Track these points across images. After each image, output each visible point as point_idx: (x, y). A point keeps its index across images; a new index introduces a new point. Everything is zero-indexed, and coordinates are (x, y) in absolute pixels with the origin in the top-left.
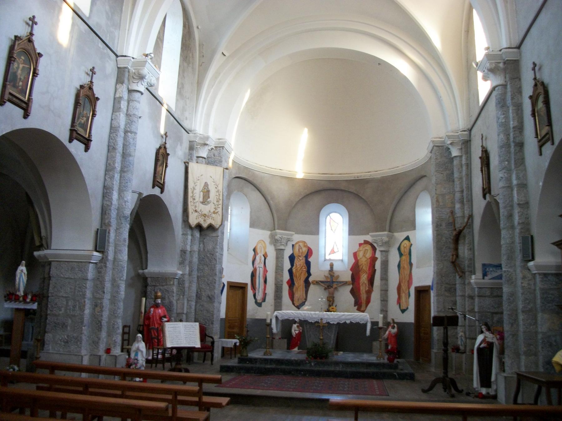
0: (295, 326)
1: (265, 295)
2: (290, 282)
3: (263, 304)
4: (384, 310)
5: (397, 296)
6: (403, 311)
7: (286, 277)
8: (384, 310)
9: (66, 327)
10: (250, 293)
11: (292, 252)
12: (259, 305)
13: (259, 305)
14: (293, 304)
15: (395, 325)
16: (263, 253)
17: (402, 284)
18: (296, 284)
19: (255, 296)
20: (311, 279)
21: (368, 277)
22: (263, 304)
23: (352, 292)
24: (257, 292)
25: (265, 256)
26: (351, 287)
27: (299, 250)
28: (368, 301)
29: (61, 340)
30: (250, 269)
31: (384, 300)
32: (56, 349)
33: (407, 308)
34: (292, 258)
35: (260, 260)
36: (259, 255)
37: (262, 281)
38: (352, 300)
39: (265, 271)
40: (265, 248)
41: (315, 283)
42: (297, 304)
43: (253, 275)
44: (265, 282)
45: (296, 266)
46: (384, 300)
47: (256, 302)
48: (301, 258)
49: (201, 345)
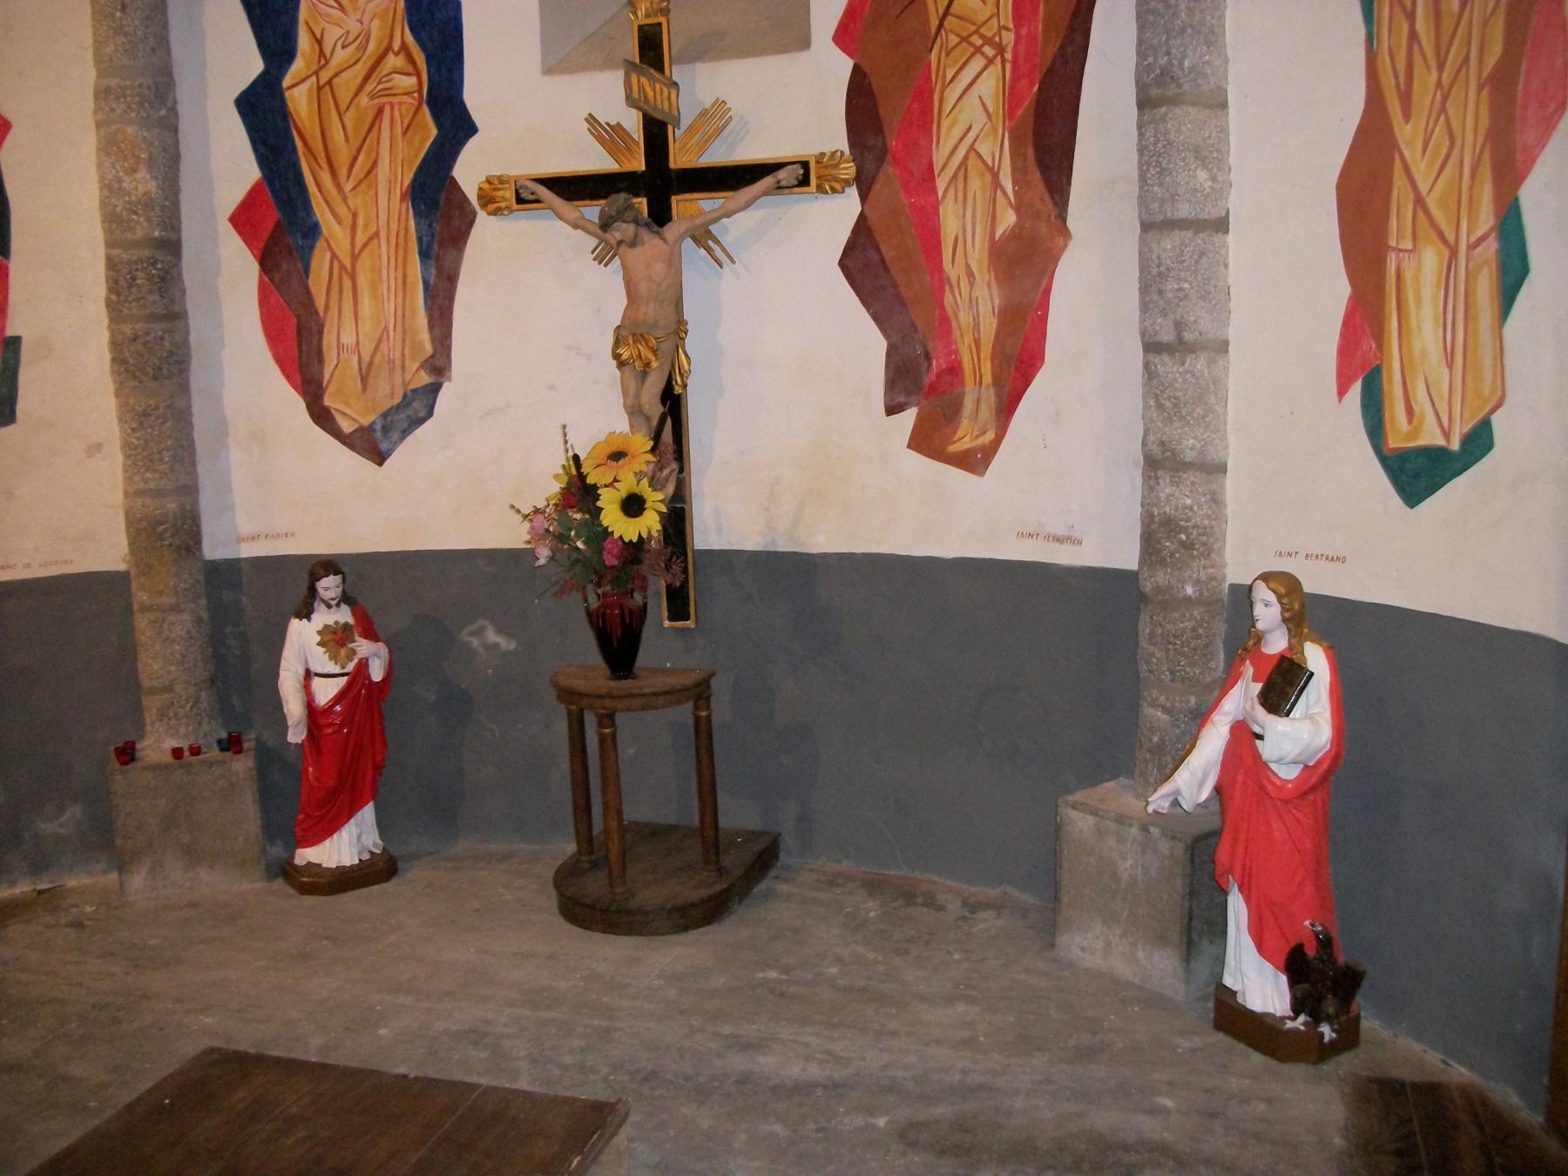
0: (303, 640)
2: (272, 216)
4: (1173, 462)
5: (1338, 290)
6: (1417, 474)
7: (227, 165)
8: (1173, 462)
14: (322, 417)
15: (1316, 658)
17: (1406, 133)
20: (469, 171)
21: (1012, 97)
23: (863, 262)
26: (846, 208)
28: (1020, 362)
31: (1175, 346)
33: (1479, 441)
38: (864, 346)
42: (352, 414)
45: (323, 57)
46: (1175, 346)
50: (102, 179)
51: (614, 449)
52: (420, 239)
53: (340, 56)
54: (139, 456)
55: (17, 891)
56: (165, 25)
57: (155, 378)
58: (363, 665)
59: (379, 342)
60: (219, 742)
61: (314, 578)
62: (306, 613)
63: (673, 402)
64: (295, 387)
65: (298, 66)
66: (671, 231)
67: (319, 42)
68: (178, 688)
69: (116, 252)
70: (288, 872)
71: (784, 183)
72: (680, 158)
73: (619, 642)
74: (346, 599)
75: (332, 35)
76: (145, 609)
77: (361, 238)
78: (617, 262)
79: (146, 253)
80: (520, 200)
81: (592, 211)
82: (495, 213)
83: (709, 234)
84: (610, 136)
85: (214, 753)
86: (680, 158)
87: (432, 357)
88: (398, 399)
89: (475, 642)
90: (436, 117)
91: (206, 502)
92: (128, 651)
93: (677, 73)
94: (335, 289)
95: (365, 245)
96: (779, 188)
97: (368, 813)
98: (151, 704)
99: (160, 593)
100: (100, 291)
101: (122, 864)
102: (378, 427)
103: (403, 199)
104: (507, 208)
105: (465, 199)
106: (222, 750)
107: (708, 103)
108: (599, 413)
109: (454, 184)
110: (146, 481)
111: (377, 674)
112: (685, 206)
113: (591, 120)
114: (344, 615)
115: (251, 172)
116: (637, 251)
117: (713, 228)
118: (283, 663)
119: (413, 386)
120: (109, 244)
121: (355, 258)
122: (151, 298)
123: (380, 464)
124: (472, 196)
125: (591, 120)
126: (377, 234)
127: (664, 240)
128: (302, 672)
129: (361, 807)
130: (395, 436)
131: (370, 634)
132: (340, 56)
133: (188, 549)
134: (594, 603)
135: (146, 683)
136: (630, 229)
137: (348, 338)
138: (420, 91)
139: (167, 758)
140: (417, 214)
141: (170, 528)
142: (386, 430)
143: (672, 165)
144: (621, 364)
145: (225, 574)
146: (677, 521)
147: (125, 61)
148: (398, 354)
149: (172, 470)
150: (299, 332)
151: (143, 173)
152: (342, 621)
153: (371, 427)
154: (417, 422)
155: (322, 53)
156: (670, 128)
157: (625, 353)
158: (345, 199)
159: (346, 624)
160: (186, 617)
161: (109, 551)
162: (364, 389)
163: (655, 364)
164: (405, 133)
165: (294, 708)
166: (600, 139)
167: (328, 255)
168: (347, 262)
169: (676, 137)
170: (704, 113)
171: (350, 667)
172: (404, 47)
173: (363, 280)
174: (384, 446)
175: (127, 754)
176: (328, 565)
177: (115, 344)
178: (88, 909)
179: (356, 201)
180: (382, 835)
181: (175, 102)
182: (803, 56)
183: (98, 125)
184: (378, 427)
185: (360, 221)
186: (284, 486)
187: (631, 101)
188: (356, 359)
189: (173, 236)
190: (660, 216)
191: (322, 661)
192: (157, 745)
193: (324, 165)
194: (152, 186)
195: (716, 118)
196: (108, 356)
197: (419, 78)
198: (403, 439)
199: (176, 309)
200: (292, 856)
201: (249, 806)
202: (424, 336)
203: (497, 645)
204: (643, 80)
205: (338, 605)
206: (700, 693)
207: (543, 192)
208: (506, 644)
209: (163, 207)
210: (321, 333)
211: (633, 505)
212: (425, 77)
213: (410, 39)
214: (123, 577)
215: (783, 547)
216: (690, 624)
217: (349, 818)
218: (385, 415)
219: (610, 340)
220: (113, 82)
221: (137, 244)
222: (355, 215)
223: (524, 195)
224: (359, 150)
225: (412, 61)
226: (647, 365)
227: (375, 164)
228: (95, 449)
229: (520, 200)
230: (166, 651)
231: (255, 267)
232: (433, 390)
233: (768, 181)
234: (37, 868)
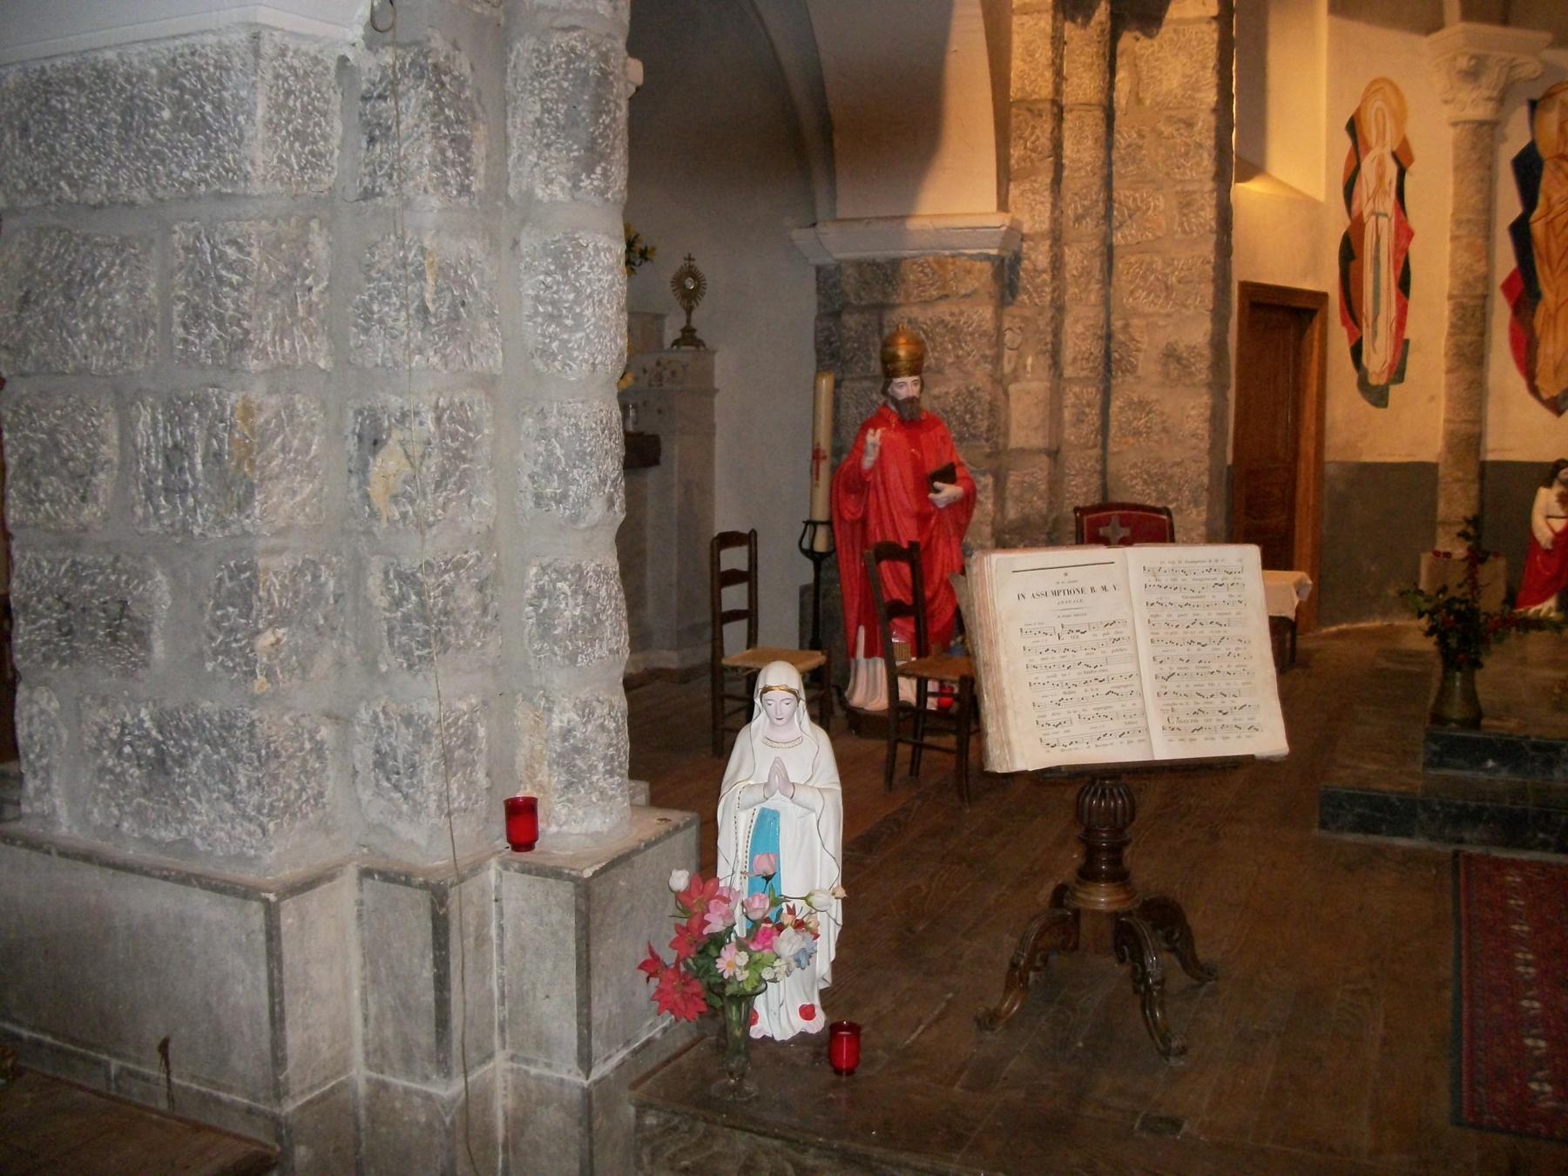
0: (1546, 498)
1: (1402, 347)
3: (1394, 390)
7: (1506, 261)
9: (141, 637)
10: (1339, 340)
12: (1378, 397)
13: (1378, 397)
14: (1534, 390)
16: (1390, 145)
19: (1357, 352)
22: (1394, 390)
24: (1366, 333)
25: (1402, 160)
29: (117, 745)
30: (1337, 224)
32: (97, 817)
34: (1528, 168)
35: (1381, 177)
39: (1404, 233)
40: (1400, 118)
42: (1549, 390)
43: (1350, 252)
44: (1404, 284)
45: (1550, 207)
47: (1363, 384)
49: (1291, 737)
62: (1549, 485)
65: (1537, 212)
75: (1556, 197)
77: (1561, 301)
121: (1557, 310)
132: (1559, 208)
137: (1550, 351)
141: (1468, 441)
161: (1431, 449)
228: (1432, 399)
234: (1385, 613)
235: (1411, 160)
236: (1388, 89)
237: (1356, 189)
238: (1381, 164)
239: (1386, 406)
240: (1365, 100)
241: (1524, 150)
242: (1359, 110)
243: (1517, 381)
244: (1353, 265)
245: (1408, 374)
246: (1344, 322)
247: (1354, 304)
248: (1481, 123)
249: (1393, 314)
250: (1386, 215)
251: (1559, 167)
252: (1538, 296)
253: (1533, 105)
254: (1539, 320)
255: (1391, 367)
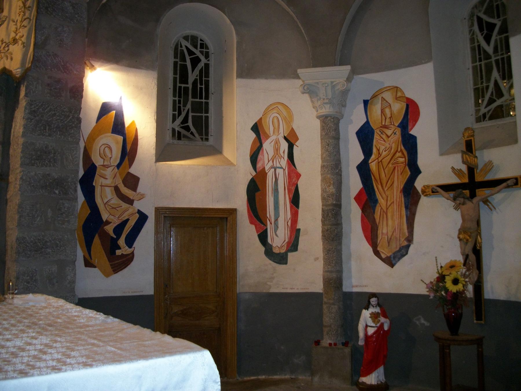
2: (365, 197)
3: (290, 254)
7: (354, 183)
10: (246, 232)
11: (365, 120)
14: (377, 253)
16: (283, 131)
18: (381, 201)
19: (263, 237)
20: (419, 184)
22: (290, 254)
25: (291, 141)
27: (382, 111)
34: (365, 136)
35: (277, 150)
36: (273, 138)
37: (284, 199)
39: (293, 174)
40: (289, 119)
41: (429, 191)
44: (295, 201)
45: (379, 154)
47: (269, 252)
48: (389, 132)
50: (322, 188)
51: (452, 264)
52: (405, 203)
53: (384, 154)
54: (327, 261)
55: (286, 377)
56: (339, 149)
57: (332, 240)
58: (382, 325)
59: (393, 232)
60: (342, 343)
61: (370, 298)
62: (367, 308)
63: (477, 252)
64: (370, 245)
65: (373, 157)
66: (475, 200)
67: (379, 150)
68: (332, 326)
69: (324, 207)
70: (357, 384)
71: (510, 185)
72: (478, 178)
73: (454, 323)
74: (379, 305)
75: (382, 148)
76: (326, 303)
77: (389, 203)
78: (459, 211)
79: (331, 207)
80: (433, 192)
81: (452, 194)
82: (426, 196)
83: (487, 201)
84: (457, 172)
85: (341, 346)
86: (478, 178)
87: (408, 237)
88: (398, 249)
89: (417, 323)
90: (409, 168)
91: (345, 275)
92: (321, 316)
93: (477, 154)
94: (382, 216)
95: (390, 205)
96: (508, 187)
97: (381, 369)
98: (326, 330)
99: (330, 299)
100: (320, 217)
101: (312, 375)
102: (392, 257)
103: (400, 192)
104: (429, 194)
105: (418, 192)
106: (343, 345)
107: (487, 161)
108: (453, 252)
109: (415, 188)
110: (328, 268)
111: (386, 328)
112: (482, 193)
113: (453, 168)
114: (378, 310)
115: (361, 186)
116: (464, 206)
117: (489, 199)
118: (360, 322)
119: (402, 245)
120: (323, 205)
121: (387, 209)
122: (332, 219)
123: (392, 267)
124: (420, 191)
125: (453, 168)
126: (393, 202)
127: (473, 203)
128: (365, 325)
129: (379, 367)
130: (397, 259)
131: (385, 316)
132: (384, 154)
133: (338, 288)
134: (446, 311)
135: (325, 324)
136: (462, 200)
137: (385, 231)
138: (405, 162)
139: (328, 345)
140: (405, 196)
142: (394, 258)
143: (476, 181)
144: (460, 240)
145: (349, 296)
146: (478, 288)
147: (328, 158)
148: (398, 236)
149: (335, 265)
150: (371, 229)
151: (331, 187)
152: (377, 311)
153: (390, 257)
154: (403, 256)
155: (379, 153)
156: (475, 170)
157: (461, 236)
158: (385, 193)
159: (378, 313)
160: (336, 306)
161: (318, 287)
162: (389, 245)
163: (470, 240)
164: (401, 174)
165: (361, 334)
166: (455, 174)
167: (380, 208)
168: (385, 210)
169: (477, 172)
170: (485, 165)
171: (378, 325)
172: (401, 150)
173: (389, 215)
174: (394, 262)
175: (317, 343)
176: (374, 295)
177: (323, 232)
178: (302, 384)
179: (388, 193)
180: (385, 378)
181: (341, 168)
182: (515, 146)
183: (322, 175)
184: (392, 257)
185: (389, 199)
186: (367, 272)
187: (464, 162)
188: (386, 237)
189: (339, 203)
190: (473, 195)
191: (370, 323)
192: (326, 342)
193: (379, 183)
194: (334, 190)
195: (489, 166)
196: (321, 234)
197: (405, 157)
198: (399, 260)
199: (339, 222)
200: (359, 378)
201: (348, 362)
202: (406, 231)
203: (424, 324)
204: (467, 156)
205: (376, 307)
206: (479, 342)
207: (439, 189)
208: (427, 324)
209: (336, 196)
210: (377, 229)
211: (456, 282)
212: (407, 158)
213: (403, 148)
214: (322, 294)
215: (513, 299)
216: (483, 322)
217: (375, 370)
218: (394, 254)
219: (457, 233)
220: (325, 164)
221: (329, 205)
222: (387, 197)
223: (434, 190)
224: (389, 179)
225: (403, 154)
226: (467, 240)
227: (393, 182)
228: (316, 259)
229: (433, 192)
230: (330, 315)
231: (360, 211)
232: (408, 247)
233: (504, 184)
235: (297, 139)
236: (280, 107)
237: (260, 156)
238: (277, 142)
239: (286, 263)
240: (265, 113)
241: (362, 127)
242: (261, 119)
243: (368, 249)
244: (257, 194)
245: (299, 247)
246: (251, 223)
247: (260, 214)
248: (326, 117)
249: (289, 215)
250: (282, 168)
251: (382, 132)
252: (376, 201)
253: (366, 103)
254: (377, 216)
255: (288, 243)
